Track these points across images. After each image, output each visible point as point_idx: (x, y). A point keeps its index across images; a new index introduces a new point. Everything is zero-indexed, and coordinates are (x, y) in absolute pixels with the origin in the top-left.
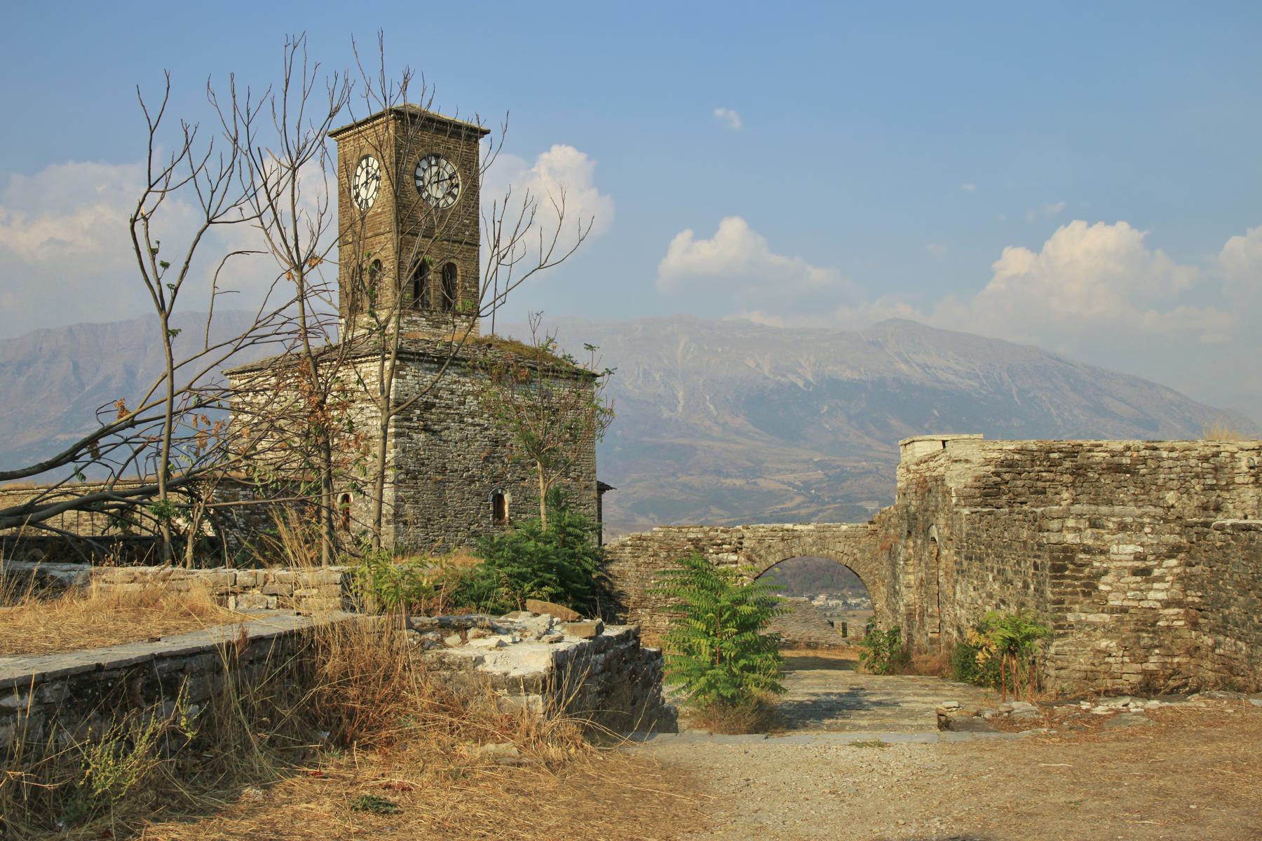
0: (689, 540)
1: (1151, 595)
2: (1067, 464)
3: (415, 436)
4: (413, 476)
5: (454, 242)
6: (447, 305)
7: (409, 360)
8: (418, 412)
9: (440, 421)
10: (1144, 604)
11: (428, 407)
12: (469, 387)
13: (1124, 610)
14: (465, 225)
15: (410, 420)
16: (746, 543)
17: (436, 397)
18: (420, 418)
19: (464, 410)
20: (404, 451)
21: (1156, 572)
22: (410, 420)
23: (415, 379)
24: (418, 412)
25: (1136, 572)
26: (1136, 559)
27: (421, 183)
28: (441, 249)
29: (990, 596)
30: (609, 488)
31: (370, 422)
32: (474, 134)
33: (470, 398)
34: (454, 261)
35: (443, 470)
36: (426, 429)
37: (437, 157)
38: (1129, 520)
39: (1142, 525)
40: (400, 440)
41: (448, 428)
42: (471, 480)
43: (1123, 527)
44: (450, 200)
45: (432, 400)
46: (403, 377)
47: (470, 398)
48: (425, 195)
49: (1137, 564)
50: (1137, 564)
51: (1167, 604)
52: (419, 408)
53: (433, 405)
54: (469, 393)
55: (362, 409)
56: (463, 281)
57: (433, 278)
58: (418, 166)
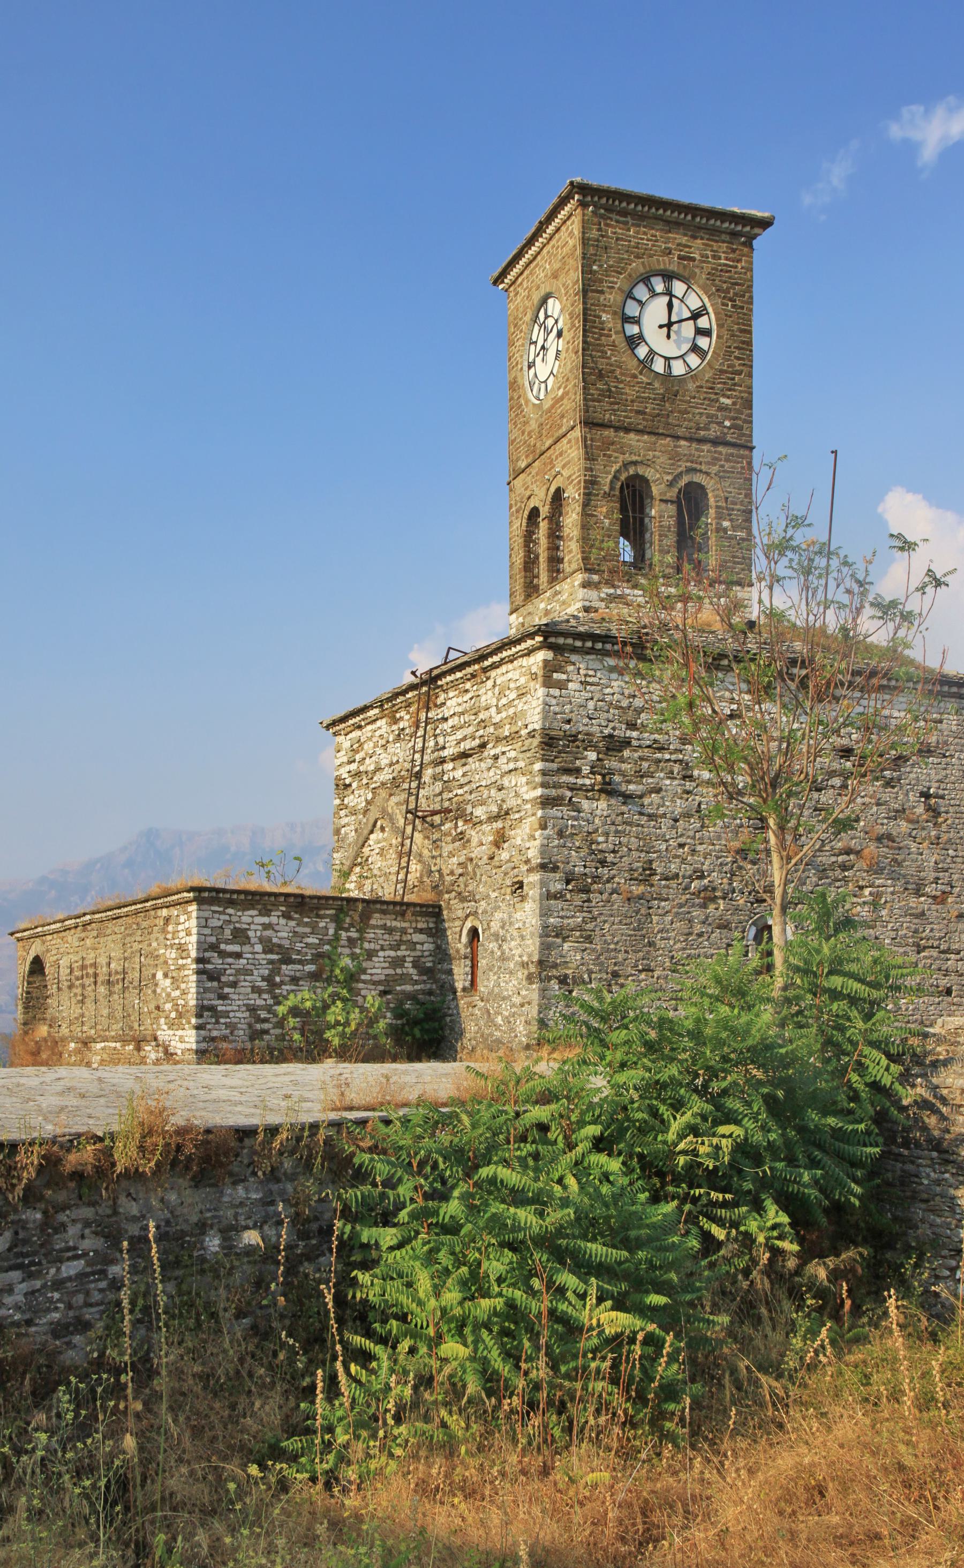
3: (585, 805)
5: (701, 441)
7: (574, 650)
8: (592, 756)
9: (641, 775)
11: (614, 745)
14: (722, 408)
15: (578, 771)
17: (632, 726)
20: (561, 834)
23: (597, 692)
24: (592, 756)
27: (635, 330)
28: (675, 457)
31: (506, 781)
32: (743, 229)
34: (698, 478)
35: (647, 874)
37: (668, 277)
40: (554, 812)
41: (658, 791)
44: (694, 360)
45: (622, 732)
46: (561, 685)
52: (595, 748)
53: (627, 743)
55: (496, 758)
56: (720, 517)
57: (660, 515)
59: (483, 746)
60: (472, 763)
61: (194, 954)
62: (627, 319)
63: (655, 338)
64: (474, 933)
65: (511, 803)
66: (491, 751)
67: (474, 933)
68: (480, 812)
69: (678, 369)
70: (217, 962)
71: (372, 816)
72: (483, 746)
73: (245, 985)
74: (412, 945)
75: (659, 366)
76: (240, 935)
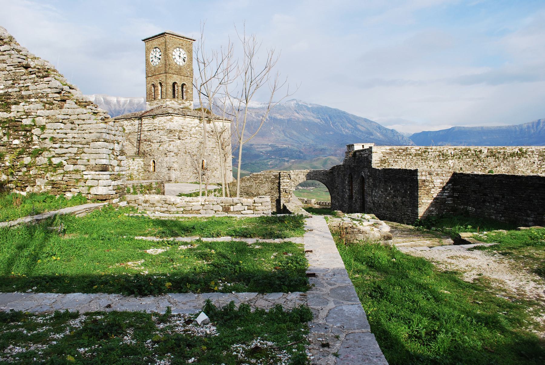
10: (443, 197)
11: (181, 131)
12: (193, 125)
19: (191, 132)
29: (389, 194)
33: (193, 129)
38: (439, 172)
43: (437, 174)
47: (193, 129)
48: (175, 61)
51: (448, 197)
54: (193, 127)
57: (178, 89)
60: (152, 132)
66: (157, 131)
68: (154, 141)
75: (178, 63)
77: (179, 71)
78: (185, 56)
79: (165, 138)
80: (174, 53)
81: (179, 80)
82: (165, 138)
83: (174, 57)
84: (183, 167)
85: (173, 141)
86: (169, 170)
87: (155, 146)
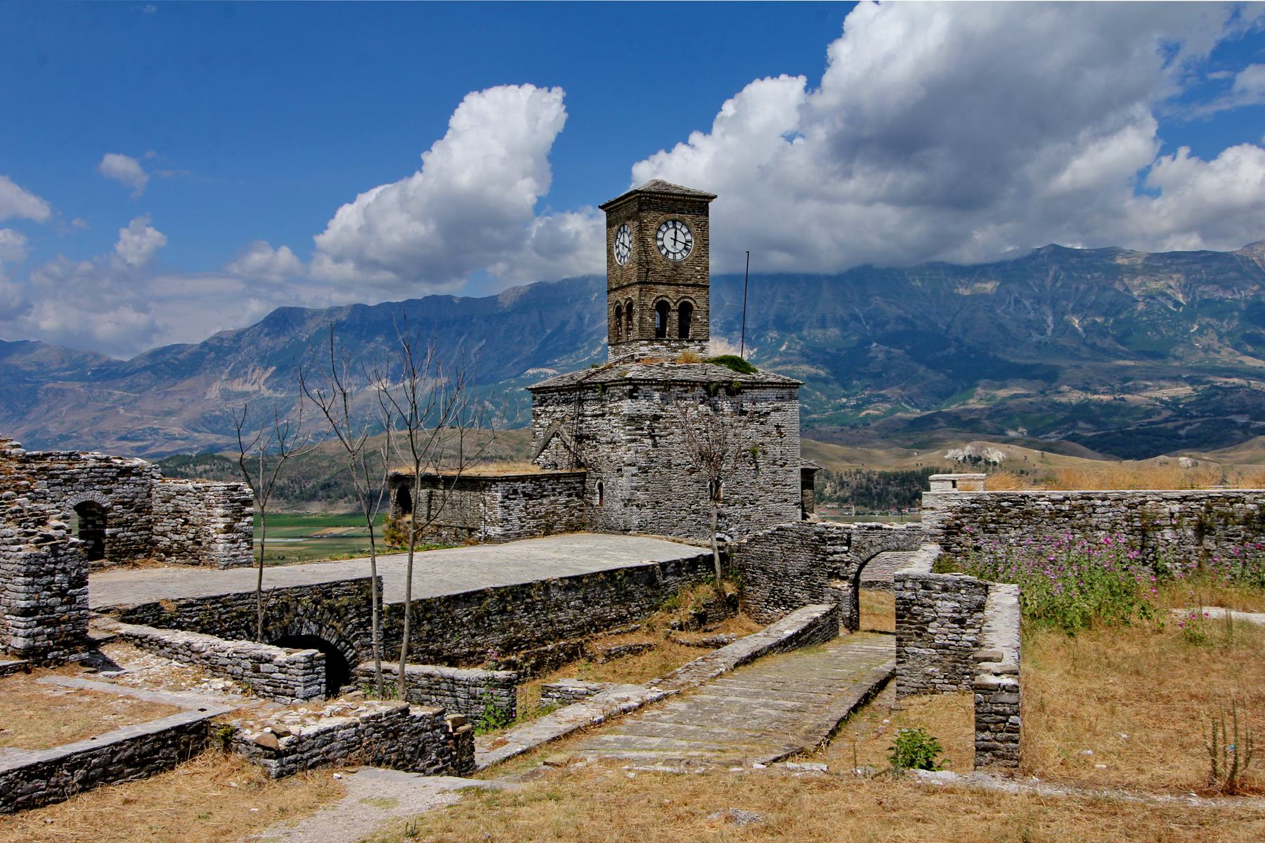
0: (816, 533)
1: (964, 637)
2: (1015, 510)
4: (644, 470)
5: (688, 286)
6: (683, 333)
9: (666, 428)
11: (656, 418)
13: (945, 647)
16: (854, 538)
17: (663, 410)
18: (650, 427)
21: (969, 621)
22: (642, 429)
25: (954, 621)
26: (954, 612)
28: (678, 292)
30: (813, 471)
36: (653, 437)
38: (949, 584)
39: (959, 589)
42: (692, 471)
43: (945, 589)
47: (691, 409)
49: (955, 615)
50: (955, 615)
53: (661, 417)
58: (659, 230)
59: (603, 415)
60: (600, 420)
61: (500, 499)
62: (657, 239)
63: (669, 244)
64: (601, 486)
65: (616, 439)
66: (607, 417)
67: (601, 486)
69: (679, 257)
70: (508, 502)
71: (552, 430)
72: (603, 415)
73: (517, 510)
74: (574, 488)
76: (515, 492)
77: (674, 277)
78: (689, 237)
79: (622, 435)
80: (660, 235)
81: (671, 294)
82: (622, 435)
83: (659, 243)
84: (661, 498)
85: (635, 441)
86: (625, 505)
87: (605, 450)
